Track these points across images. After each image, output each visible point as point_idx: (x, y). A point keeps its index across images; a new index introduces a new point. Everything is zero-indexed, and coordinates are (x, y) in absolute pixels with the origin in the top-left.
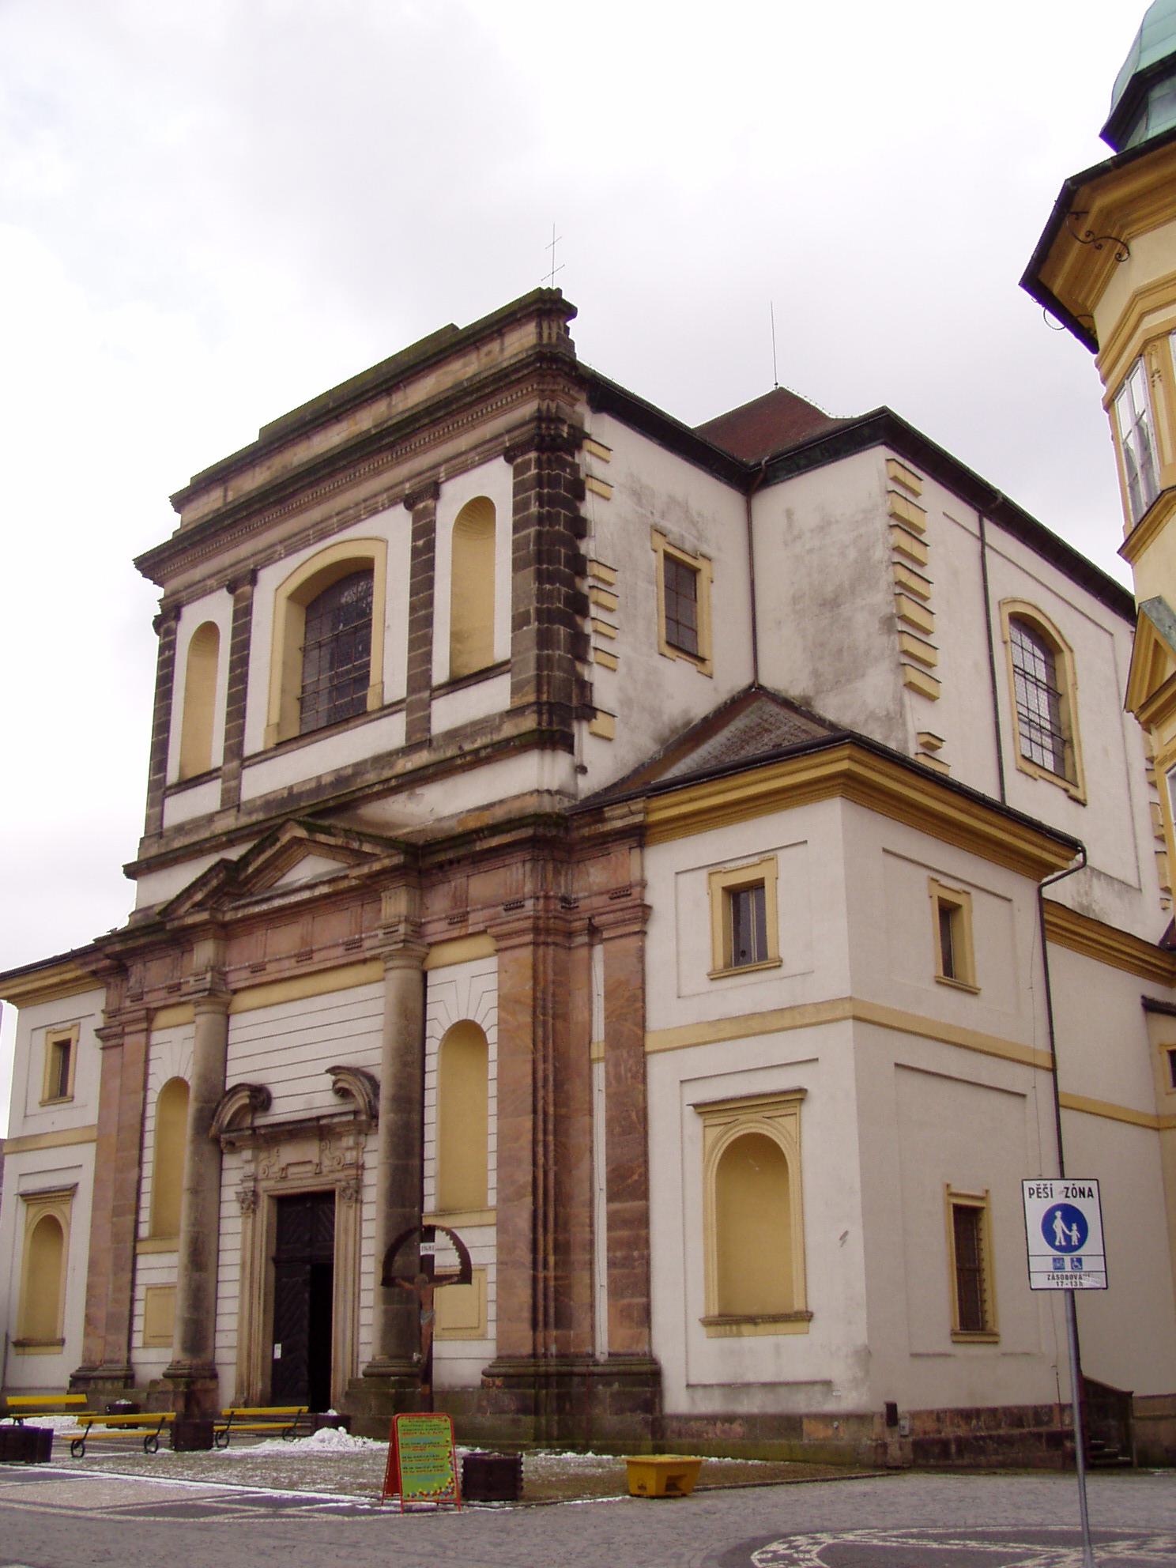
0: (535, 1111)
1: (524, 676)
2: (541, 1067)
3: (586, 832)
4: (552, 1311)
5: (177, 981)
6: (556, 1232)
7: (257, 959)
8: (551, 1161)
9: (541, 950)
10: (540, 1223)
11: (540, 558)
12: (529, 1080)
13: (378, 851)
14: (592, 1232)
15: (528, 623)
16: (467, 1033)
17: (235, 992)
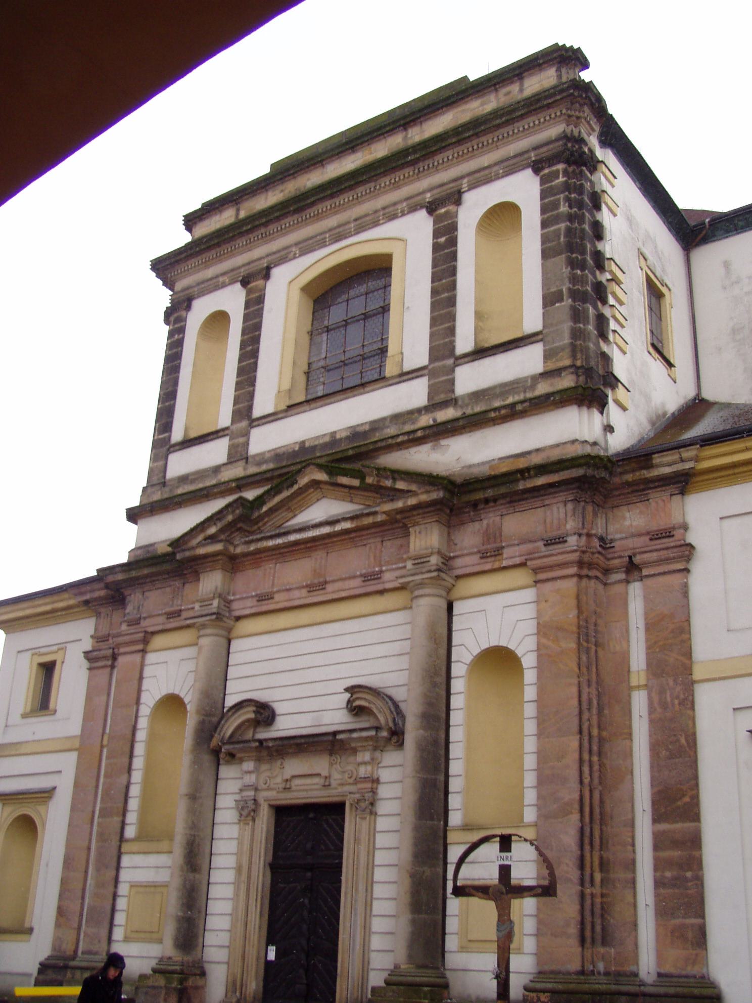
0: (581, 732)
1: (557, 344)
2: (585, 690)
3: (629, 477)
4: (598, 928)
5: (178, 608)
6: (601, 849)
7: (265, 588)
8: (596, 781)
9: (585, 582)
10: (587, 840)
11: (571, 247)
12: (575, 702)
13: (414, 487)
14: (634, 852)
15: (561, 300)
17: (238, 618)
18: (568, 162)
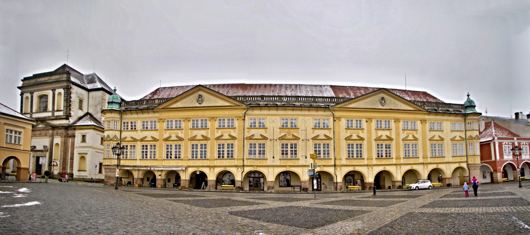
7: (35, 134)
16: (57, 144)
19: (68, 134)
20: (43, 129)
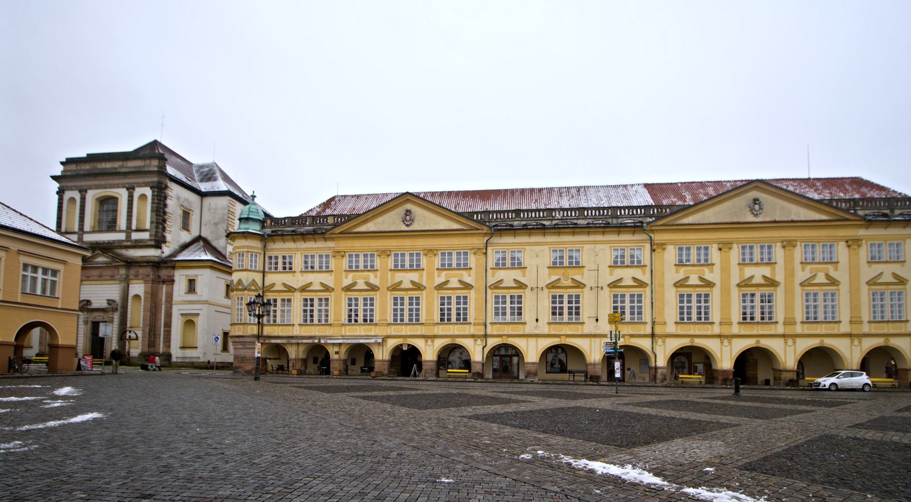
16: (137, 297)
18: (158, 189)
19: (159, 277)
20: (107, 266)
